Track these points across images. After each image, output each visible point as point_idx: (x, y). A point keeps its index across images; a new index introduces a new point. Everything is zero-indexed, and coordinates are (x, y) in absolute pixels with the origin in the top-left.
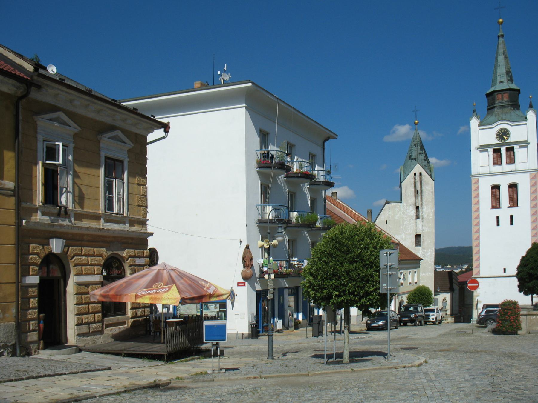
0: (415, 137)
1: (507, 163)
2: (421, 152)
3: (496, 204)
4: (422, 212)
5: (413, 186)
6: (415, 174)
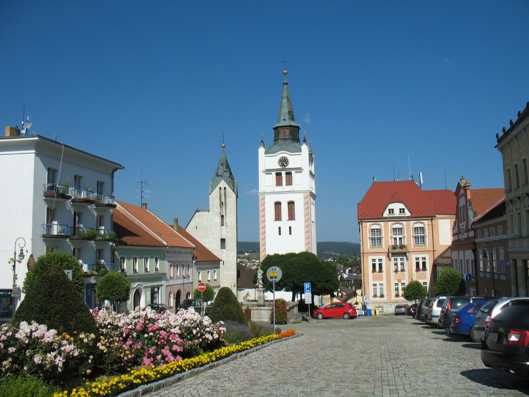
0: (222, 158)
1: (287, 185)
2: (227, 170)
3: (278, 217)
4: (226, 220)
5: (219, 198)
6: (220, 188)
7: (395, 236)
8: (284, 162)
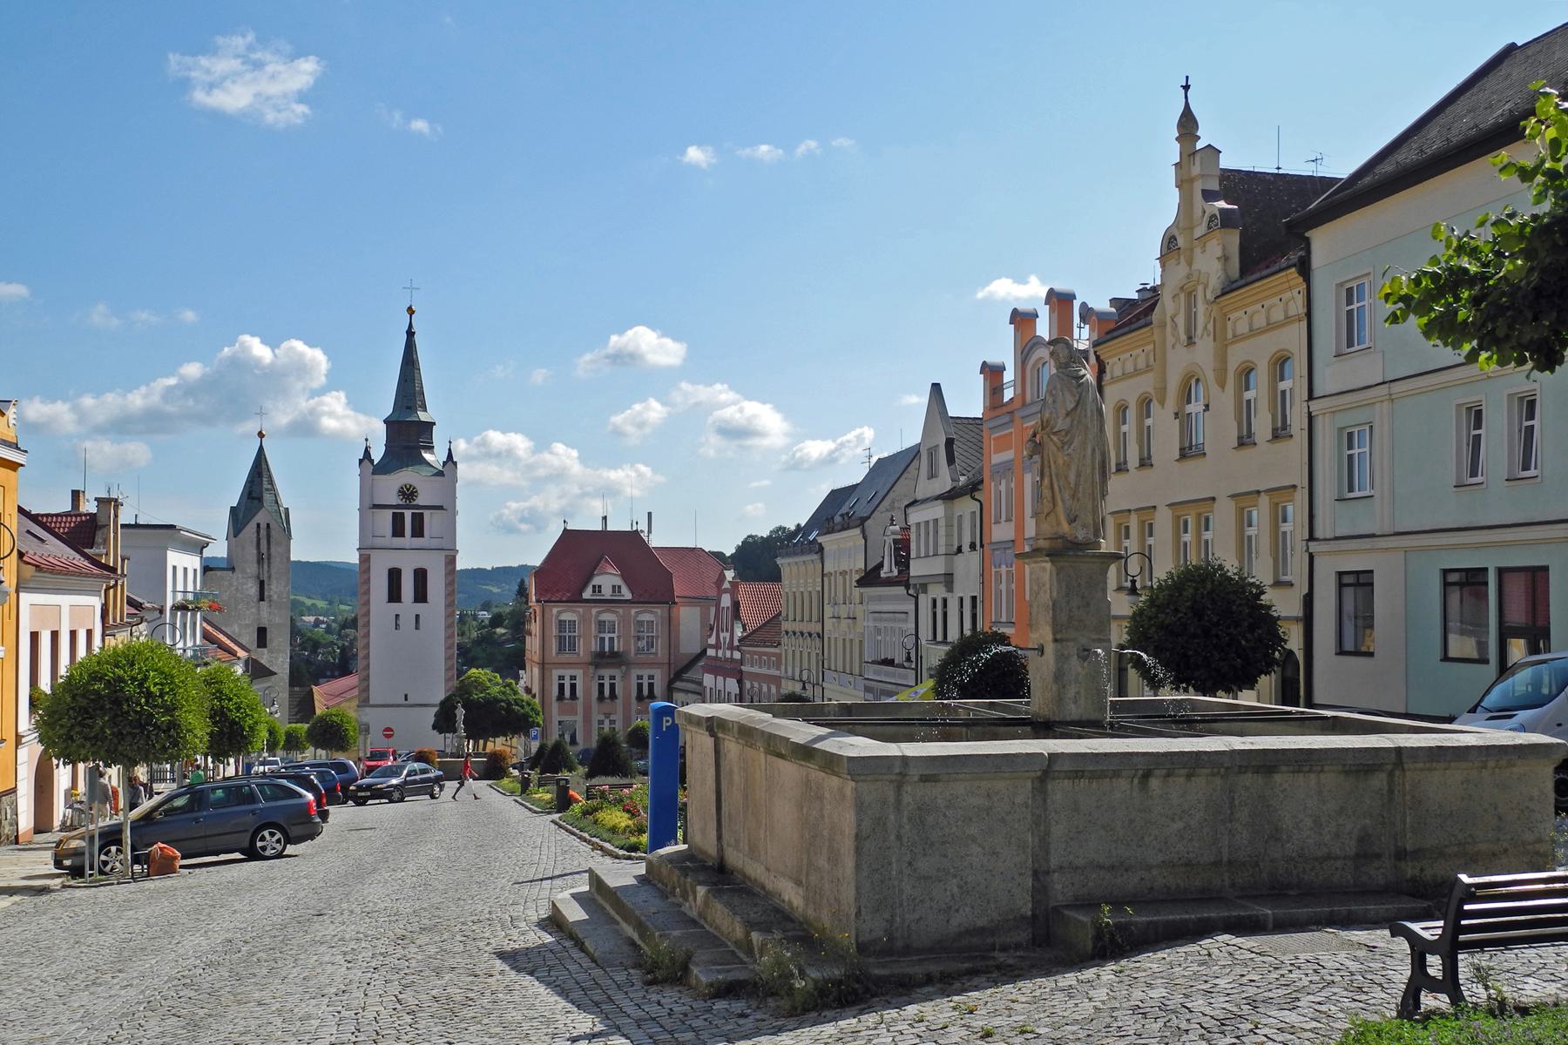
3: (394, 595)
5: (255, 544)
6: (258, 525)
7: (602, 635)
8: (408, 493)
